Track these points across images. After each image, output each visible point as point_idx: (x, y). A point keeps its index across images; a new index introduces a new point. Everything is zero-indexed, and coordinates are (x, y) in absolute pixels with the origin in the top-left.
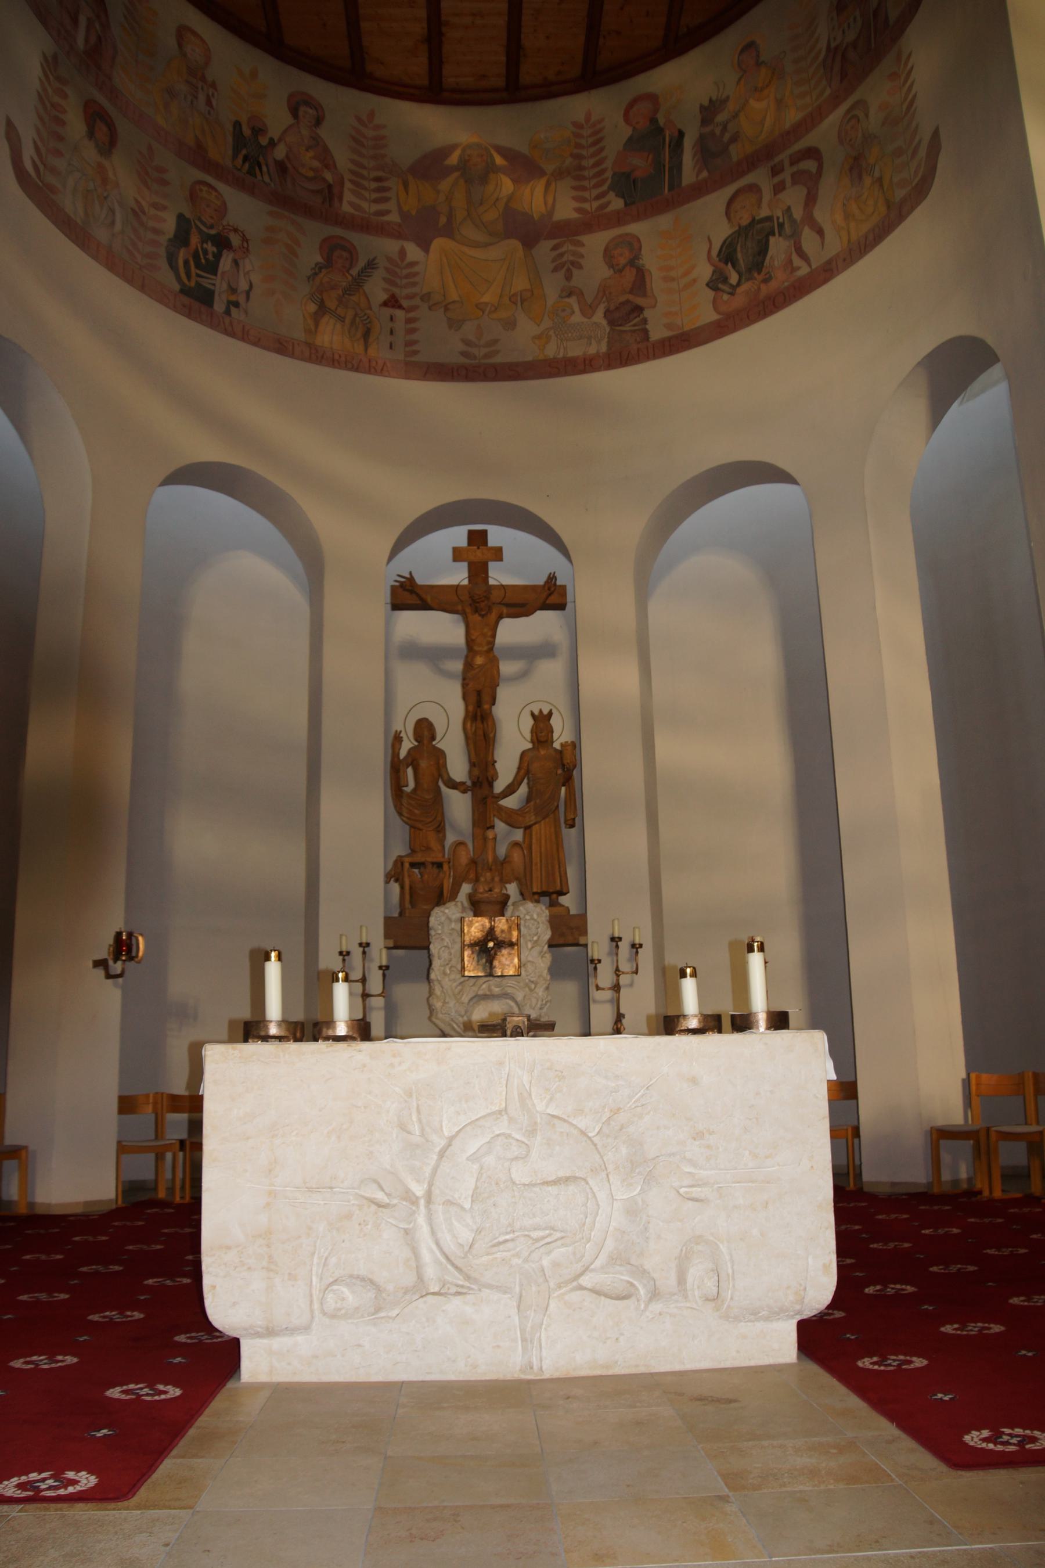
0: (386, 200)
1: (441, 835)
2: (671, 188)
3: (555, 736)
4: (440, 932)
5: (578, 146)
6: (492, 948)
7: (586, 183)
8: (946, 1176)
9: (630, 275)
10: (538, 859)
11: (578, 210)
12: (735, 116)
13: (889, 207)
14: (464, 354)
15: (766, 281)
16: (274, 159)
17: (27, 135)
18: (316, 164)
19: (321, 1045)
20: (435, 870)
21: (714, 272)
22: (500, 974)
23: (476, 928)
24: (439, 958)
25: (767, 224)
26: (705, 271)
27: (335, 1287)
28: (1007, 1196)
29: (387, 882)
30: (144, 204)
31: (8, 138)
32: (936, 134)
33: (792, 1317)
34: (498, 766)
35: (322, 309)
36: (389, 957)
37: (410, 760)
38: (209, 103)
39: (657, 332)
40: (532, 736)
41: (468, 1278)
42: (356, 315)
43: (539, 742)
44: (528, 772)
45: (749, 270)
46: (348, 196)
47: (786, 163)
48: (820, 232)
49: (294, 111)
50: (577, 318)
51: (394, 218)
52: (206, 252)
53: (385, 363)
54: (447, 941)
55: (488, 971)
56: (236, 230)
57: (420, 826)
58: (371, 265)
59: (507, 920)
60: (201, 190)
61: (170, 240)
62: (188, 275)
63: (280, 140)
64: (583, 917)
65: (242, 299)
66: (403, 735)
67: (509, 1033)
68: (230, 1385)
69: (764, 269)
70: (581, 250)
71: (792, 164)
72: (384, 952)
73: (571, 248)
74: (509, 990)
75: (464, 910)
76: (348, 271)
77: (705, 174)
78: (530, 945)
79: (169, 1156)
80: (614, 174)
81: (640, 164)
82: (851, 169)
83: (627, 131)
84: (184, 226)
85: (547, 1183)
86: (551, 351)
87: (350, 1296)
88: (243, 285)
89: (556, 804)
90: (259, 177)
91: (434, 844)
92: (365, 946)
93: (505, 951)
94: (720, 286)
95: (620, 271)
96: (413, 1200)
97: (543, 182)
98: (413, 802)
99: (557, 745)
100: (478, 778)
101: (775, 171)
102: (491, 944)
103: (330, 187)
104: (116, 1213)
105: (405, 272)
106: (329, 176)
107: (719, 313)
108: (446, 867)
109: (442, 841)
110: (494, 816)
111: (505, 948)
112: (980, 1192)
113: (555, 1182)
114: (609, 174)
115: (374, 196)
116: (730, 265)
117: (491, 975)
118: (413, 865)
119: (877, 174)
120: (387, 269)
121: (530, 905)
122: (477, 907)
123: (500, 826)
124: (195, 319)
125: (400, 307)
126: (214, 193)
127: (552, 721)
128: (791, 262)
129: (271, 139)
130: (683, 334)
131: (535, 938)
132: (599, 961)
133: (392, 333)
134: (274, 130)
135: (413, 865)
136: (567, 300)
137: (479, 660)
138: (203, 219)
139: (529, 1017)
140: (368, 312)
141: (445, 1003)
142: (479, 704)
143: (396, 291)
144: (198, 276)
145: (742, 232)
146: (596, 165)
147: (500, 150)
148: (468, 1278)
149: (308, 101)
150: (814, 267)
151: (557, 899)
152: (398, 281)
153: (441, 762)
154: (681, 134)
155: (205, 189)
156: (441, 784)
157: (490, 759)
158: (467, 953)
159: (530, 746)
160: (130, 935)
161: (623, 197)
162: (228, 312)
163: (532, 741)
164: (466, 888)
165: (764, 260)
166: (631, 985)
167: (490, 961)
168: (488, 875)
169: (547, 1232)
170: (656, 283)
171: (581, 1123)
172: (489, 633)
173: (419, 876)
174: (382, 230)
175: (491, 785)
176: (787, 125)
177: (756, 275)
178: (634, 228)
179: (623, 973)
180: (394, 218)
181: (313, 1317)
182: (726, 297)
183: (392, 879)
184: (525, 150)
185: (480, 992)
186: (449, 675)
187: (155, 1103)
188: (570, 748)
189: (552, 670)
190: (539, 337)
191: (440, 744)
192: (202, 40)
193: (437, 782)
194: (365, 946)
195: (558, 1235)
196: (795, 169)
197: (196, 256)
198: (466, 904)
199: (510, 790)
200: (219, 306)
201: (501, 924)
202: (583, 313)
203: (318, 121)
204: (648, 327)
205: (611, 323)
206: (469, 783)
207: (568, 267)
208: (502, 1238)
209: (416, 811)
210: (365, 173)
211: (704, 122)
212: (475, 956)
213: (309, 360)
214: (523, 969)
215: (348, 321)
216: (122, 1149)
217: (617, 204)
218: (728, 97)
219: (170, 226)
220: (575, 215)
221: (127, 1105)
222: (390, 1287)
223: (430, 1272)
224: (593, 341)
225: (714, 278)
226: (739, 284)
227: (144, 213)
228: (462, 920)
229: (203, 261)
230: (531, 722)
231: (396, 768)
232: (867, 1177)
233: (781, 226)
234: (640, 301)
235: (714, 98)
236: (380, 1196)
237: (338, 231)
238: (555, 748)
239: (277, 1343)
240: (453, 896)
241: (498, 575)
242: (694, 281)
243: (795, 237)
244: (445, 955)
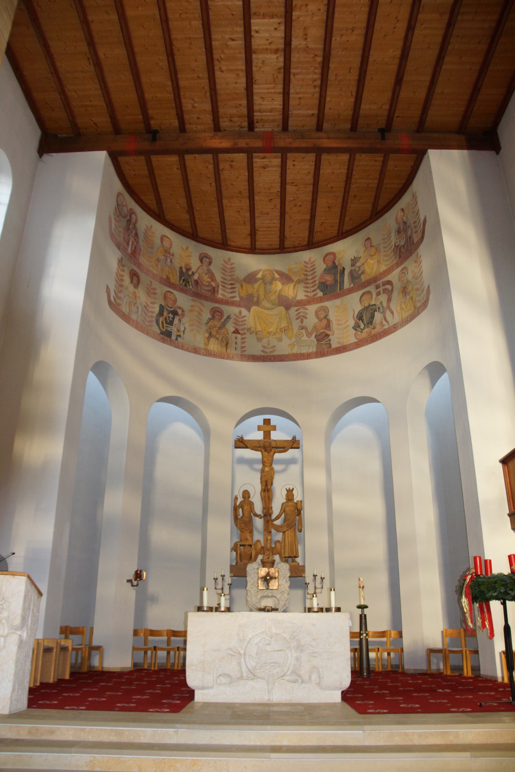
0: (235, 292)
1: (251, 534)
2: (340, 290)
3: (295, 497)
4: (250, 573)
5: (306, 271)
6: (269, 579)
7: (309, 285)
8: (434, 667)
9: (325, 322)
10: (288, 544)
11: (306, 296)
12: (363, 264)
13: (415, 308)
14: (263, 351)
15: (374, 328)
16: (194, 280)
17: (112, 289)
18: (209, 280)
19: (217, 613)
20: (249, 548)
21: (355, 323)
22: (271, 589)
23: (263, 571)
24: (250, 582)
25: (374, 307)
26: (352, 323)
27: (220, 677)
28: (452, 674)
29: (231, 551)
30: (148, 302)
31: (107, 292)
32: (429, 287)
33: (340, 689)
34: (273, 509)
35: (211, 335)
36: (232, 580)
37: (240, 506)
38: (171, 262)
39: (334, 345)
40: (286, 497)
41: (254, 675)
42: (223, 337)
43: (289, 500)
44: (284, 511)
45: (368, 324)
46: (220, 291)
47: (381, 285)
48: (392, 313)
49: (201, 261)
50: (305, 338)
51: (237, 299)
52: (169, 317)
53: (233, 355)
54: (253, 576)
55: (267, 587)
56: (180, 308)
57: (243, 530)
58: (229, 317)
59: (274, 569)
60: (168, 294)
61: (157, 315)
62: (163, 328)
63: (196, 272)
64: (304, 566)
65: (182, 334)
66: (238, 496)
67: (266, 611)
68: (192, 702)
69: (373, 324)
70: (307, 311)
71: (383, 286)
72: (230, 579)
73: (303, 310)
74: (274, 594)
75: (259, 565)
76: (220, 320)
77: (352, 285)
78: (282, 578)
79: (149, 652)
80: (319, 282)
81: (329, 279)
82: (402, 292)
83: (324, 266)
84: (162, 308)
85: (275, 651)
86: (295, 350)
87: (223, 680)
88: (182, 329)
89: (294, 524)
90: (188, 287)
91: (249, 537)
92: (223, 576)
93: (273, 581)
94: (357, 328)
95: (321, 320)
96: (241, 655)
97: (293, 284)
98: (241, 522)
99: (295, 501)
100: (266, 514)
101: (377, 287)
102: (268, 578)
103: (214, 288)
104: (130, 673)
105: (241, 320)
106: (213, 284)
107: (357, 339)
108: (253, 546)
109: (252, 537)
110: (271, 528)
111: (273, 579)
112: (443, 673)
113: (278, 651)
114: (317, 282)
115: (230, 290)
116: (361, 321)
117: (268, 589)
118: (241, 545)
119: (411, 296)
120: (234, 319)
121: (283, 564)
122: (264, 564)
123: (273, 531)
124: (165, 343)
125: (239, 333)
126: (173, 295)
127: (294, 492)
128: (382, 322)
129: (193, 272)
130: (344, 346)
131: (284, 576)
132: (309, 584)
133: (236, 343)
134: (194, 269)
135: (241, 545)
136: (301, 331)
137: (267, 469)
138: (168, 305)
139: (271, 607)
140: (227, 336)
141: (251, 598)
142: (266, 485)
143: (238, 327)
144: (167, 327)
145: (366, 309)
146: (313, 278)
147: (277, 271)
148: (254, 675)
149: (206, 256)
150: (390, 326)
151: (295, 559)
152: (238, 323)
153: (252, 506)
154: (344, 269)
155: (169, 294)
156: (252, 514)
157: (270, 506)
158: (260, 581)
159: (285, 501)
160: (141, 571)
161: (322, 291)
162: (177, 339)
163: (286, 499)
164: (260, 557)
165: (373, 320)
166: (321, 593)
167: (268, 584)
168: (268, 552)
169: (275, 664)
170: (334, 326)
171: (285, 635)
172: (271, 459)
173: (243, 550)
174: (233, 304)
175: (270, 516)
176: (381, 271)
177: (370, 326)
178: (326, 304)
179: (317, 588)
180: (237, 299)
181: (214, 685)
182: (359, 333)
183: (233, 550)
184: (286, 272)
185: (264, 595)
186: (256, 470)
187: (144, 633)
188: (300, 503)
189: (294, 469)
190: (291, 345)
191: (251, 499)
192: (169, 239)
193: (251, 514)
194: (223, 576)
195: (278, 665)
196: (384, 287)
197: (166, 319)
198: (260, 562)
199: (278, 518)
200: (174, 337)
201: (272, 570)
202: (307, 336)
203: (210, 263)
204: (331, 342)
205: (318, 340)
206: (262, 515)
207: (301, 318)
208: (263, 665)
209: (243, 525)
210: (226, 282)
211: (353, 265)
212: (263, 581)
213: (206, 355)
214: (279, 587)
215: (220, 339)
216: (134, 649)
217: (320, 294)
218: (361, 257)
219: (157, 310)
220: (305, 298)
221: (136, 633)
222: (234, 677)
223: (245, 674)
224: (311, 347)
225: (355, 325)
226: (364, 329)
227: (148, 306)
228: (258, 569)
229: (168, 321)
230: (286, 492)
231: (235, 509)
232: (406, 667)
233: (379, 308)
234: (328, 332)
235: (356, 257)
236: (232, 653)
237: (216, 305)
238: (294, 502)
239: (205, 691)
240: (255, 560)
241: (275, 436)
242: (348, 326)
243: (384, 313)
244: (252, 581)
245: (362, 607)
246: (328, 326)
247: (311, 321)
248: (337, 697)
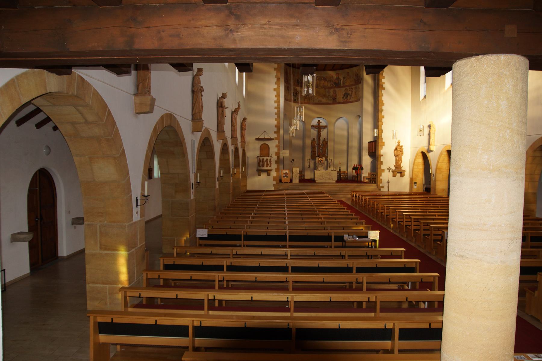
9: (335, 95)
26: (342, 96)
39: (337, 102)
48: (352, 97)
101: (349, 88)
147: (323, 77)
154: (341, 80)
178: (336, 89)
186: (316, 131)
201: (322, 159)
205: (333, 100)
207: (329, 92)
211: (344, 79)
217: (334, 86)
234: (336, 98)
241: (321, 124)
245: (340, 167)
246: (336, 96)
247: (332, 93)
248: (335, 182)
